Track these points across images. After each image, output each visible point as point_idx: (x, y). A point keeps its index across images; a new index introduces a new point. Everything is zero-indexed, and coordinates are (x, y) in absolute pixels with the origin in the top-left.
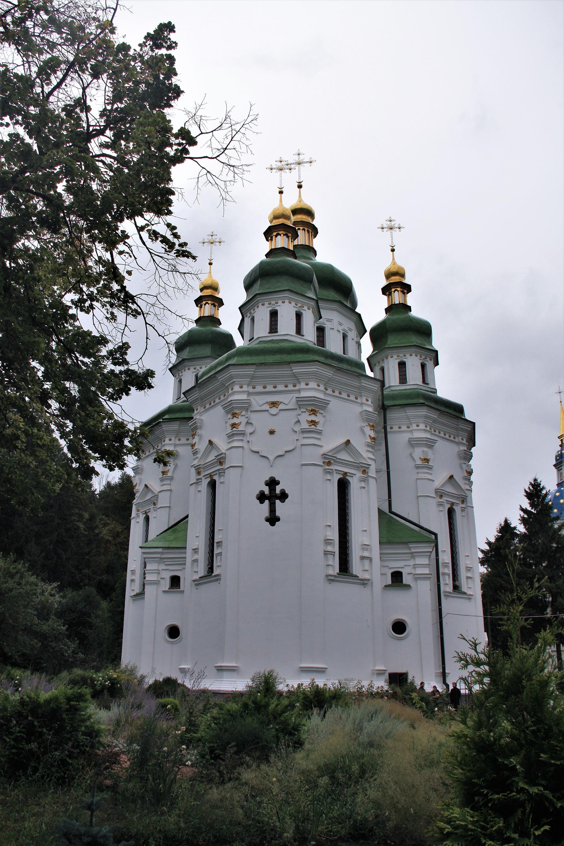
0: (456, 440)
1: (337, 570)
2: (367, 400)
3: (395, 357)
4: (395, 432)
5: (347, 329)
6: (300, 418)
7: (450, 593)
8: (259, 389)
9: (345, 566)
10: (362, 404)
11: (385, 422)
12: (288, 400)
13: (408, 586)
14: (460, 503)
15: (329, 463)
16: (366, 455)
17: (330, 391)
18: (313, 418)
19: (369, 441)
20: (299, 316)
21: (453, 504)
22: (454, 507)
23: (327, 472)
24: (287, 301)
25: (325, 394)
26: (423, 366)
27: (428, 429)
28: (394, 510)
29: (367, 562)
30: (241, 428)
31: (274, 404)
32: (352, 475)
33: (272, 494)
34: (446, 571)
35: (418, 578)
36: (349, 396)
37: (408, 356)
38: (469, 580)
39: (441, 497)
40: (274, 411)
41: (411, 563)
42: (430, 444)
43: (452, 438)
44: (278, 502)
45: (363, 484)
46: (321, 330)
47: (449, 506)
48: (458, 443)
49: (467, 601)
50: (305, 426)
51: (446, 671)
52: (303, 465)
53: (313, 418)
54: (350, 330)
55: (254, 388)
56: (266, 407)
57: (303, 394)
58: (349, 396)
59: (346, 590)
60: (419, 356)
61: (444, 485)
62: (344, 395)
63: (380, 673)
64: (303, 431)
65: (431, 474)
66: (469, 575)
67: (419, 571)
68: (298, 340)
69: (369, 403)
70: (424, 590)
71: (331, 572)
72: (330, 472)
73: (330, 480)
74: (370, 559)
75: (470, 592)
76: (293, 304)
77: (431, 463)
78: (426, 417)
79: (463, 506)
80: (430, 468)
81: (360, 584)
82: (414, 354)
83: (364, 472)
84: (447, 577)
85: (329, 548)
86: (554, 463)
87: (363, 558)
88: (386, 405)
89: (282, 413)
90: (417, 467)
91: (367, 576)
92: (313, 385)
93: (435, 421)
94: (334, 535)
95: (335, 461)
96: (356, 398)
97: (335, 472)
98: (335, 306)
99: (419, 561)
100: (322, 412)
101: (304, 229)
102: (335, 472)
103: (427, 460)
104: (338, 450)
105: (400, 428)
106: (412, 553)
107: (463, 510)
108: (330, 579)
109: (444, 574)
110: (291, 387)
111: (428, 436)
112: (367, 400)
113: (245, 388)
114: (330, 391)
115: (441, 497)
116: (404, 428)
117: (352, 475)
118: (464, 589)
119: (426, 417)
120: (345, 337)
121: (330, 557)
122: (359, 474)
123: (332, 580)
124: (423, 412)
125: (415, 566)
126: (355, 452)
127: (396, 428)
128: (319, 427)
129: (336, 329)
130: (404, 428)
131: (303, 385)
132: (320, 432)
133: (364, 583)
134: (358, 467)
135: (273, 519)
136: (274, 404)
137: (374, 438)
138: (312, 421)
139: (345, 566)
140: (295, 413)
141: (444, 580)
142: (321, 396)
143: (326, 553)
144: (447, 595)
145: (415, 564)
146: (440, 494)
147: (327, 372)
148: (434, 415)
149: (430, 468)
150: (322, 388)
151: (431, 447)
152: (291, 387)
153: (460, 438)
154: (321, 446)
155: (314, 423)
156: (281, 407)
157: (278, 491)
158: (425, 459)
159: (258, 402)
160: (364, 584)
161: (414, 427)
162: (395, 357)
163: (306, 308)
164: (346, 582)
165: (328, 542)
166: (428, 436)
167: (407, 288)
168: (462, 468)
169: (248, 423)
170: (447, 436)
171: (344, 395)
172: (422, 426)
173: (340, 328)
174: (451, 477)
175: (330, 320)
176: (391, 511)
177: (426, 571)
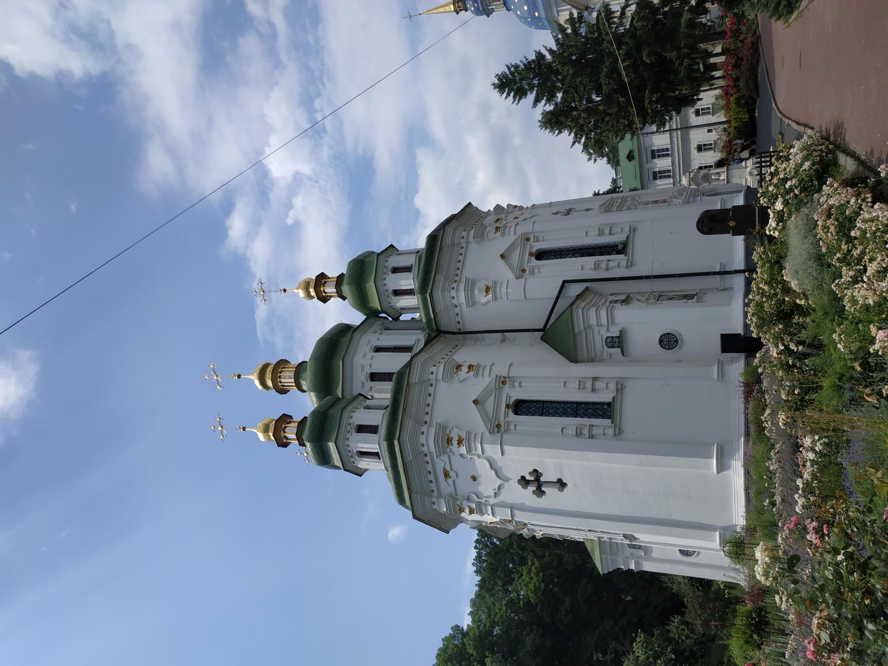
0: (464, 245)
1: (608, 422)
2: (432, 373)
3: (389, 299)
4: (462, 319)
5: (368, 349)
6: (457, 454)
7: (628, 260)
8: (433, 486)
9: (602, 410)
10: (437, 380)
11: (453, 333)
12: (441, 464)
13: (621, 331)
14: (529, 243)
15: (498, 426)
16: (487, 380)
17: (427, 418)
18: (455, 442)
19: (472, 373)
20: (361, 429)
21: (531, 254)
22: (534, 251)
23: (507, 430)
24: (347, 443)
25: (430, 426)
26: (395, 270)
27: (455, 285)
28: (542, 327)
29: (599, 385)
30: (473, 506)
31: (446, 475)
32: (509, 397)
33: (535, 482)
34: (603, 265)
35: (611, 320)
36: (430, 395)
37: (386, 288)
38: (614, 230)
39: (524, 271)
40: (452, 474)
41: (596, 329)
42: (471, 285)
43: (462, 251)
44: (542, 479)
45: (517, 384)
46: (375, 377)
47: (533, 258)
48: (468, 243)
49: (637, 233)
50: (463, 450)
51: (718, 270)
52: (502, 454)
53: (455, 442)
54: (369, 342)
55: (433, 491)
56: (450, 481)
57: (433, 449)
58: (430, 395)
59: (632, 410)
60: (385, 276)
61: (510, 266)
62: (430, 400)
63: (722, 374)
64: (469, 450)
65: (501, 283)
66: (607, 232)
67: (604, 321)
68: (383, 431)
69: (434, 369)
70: (625, 316)
71: (610, 431)
72: (508, 424)
73: (515, 426)
74: (595, 379)
75: (627, 230)
76: (348, 435)
77: (490, 285)
78: (443, 291)
79: (532, 240)
80: (495, 283)
81: (622, 393)
82: (384, 282)
83: (504, 383)
84: (611, 264)
85: (586, 431)
86: (485, 16)
87: (594, 390)
88: (436, 332)
89: (454, 468)
90: (495, 298)
91: (612, 386)
92: (422, 439)
93: (446, 278)
94: (572, 423)
95: (495, 419)
96: (431, 385)
97: (508, 419)
98: (348, 360)
99: (593, 321)
100: (448, 432)
101: (280, 377)
102: (508, 419)
103: (487, 289)
104: (484, 414)
105: (457, 315)
106: (585, 328)
107: (537, 240)
108: (618, 432)
109: (607, 269)
110: (428, 459)
111: (462, 285)
112: (432, 373)
113: (434, 500)
114: (427, 418)
115: (524, 271)
116: (457, 310)
117: (509, 397)
118: (621, 238)
119: (443, 291)
120: (378, 349)
121: (596, 431)
122: (507, 389)
123: (620, 429)
124: (438, 295)
125: (599, 325)
126: (485, 394)
127: (458, 318)
128: (464, 436)
129: (370, 362)
130: (457, 310)
131: (424, 449)
132: (469, 434)
133: (620, 389)
134: (500, 389)
135: (561, 484)
136: (446, 475)
137: (470, 367)
138: (459, 444)
139: (602, 410)
140: (452, 457)
141: (614, 267)
142: (433, 431)
143: (591, 436)
144: (630, 264)
145: (596, 322)
146: (521, 272)
147: (409, 424)
148: (440, 280)
149: (495, 283)
150: (424, 429)
151: (473, 283)
152: (428, 459)
153: (462, 240)
154: (482, 434)
155: (460, 442)
156: (448, 469)
157: (532, 479)
158: (487, 291)
159: (446, 487)
160: (622, 389)
161: (455, 301)
162: (389, 299)
163: (351, 421)
164: (621, 411)
165: (579, 434)
166: (462, 285)
167: (321, 279)
168: (493, 239)
169: (468, 499)
170: (461, 258)
171: (430, 400)
172: (453, 293)
173: (369, 356)
174: (502, 256)
175: (363, 368)
176: (543, 330)
177: (603, 313)
